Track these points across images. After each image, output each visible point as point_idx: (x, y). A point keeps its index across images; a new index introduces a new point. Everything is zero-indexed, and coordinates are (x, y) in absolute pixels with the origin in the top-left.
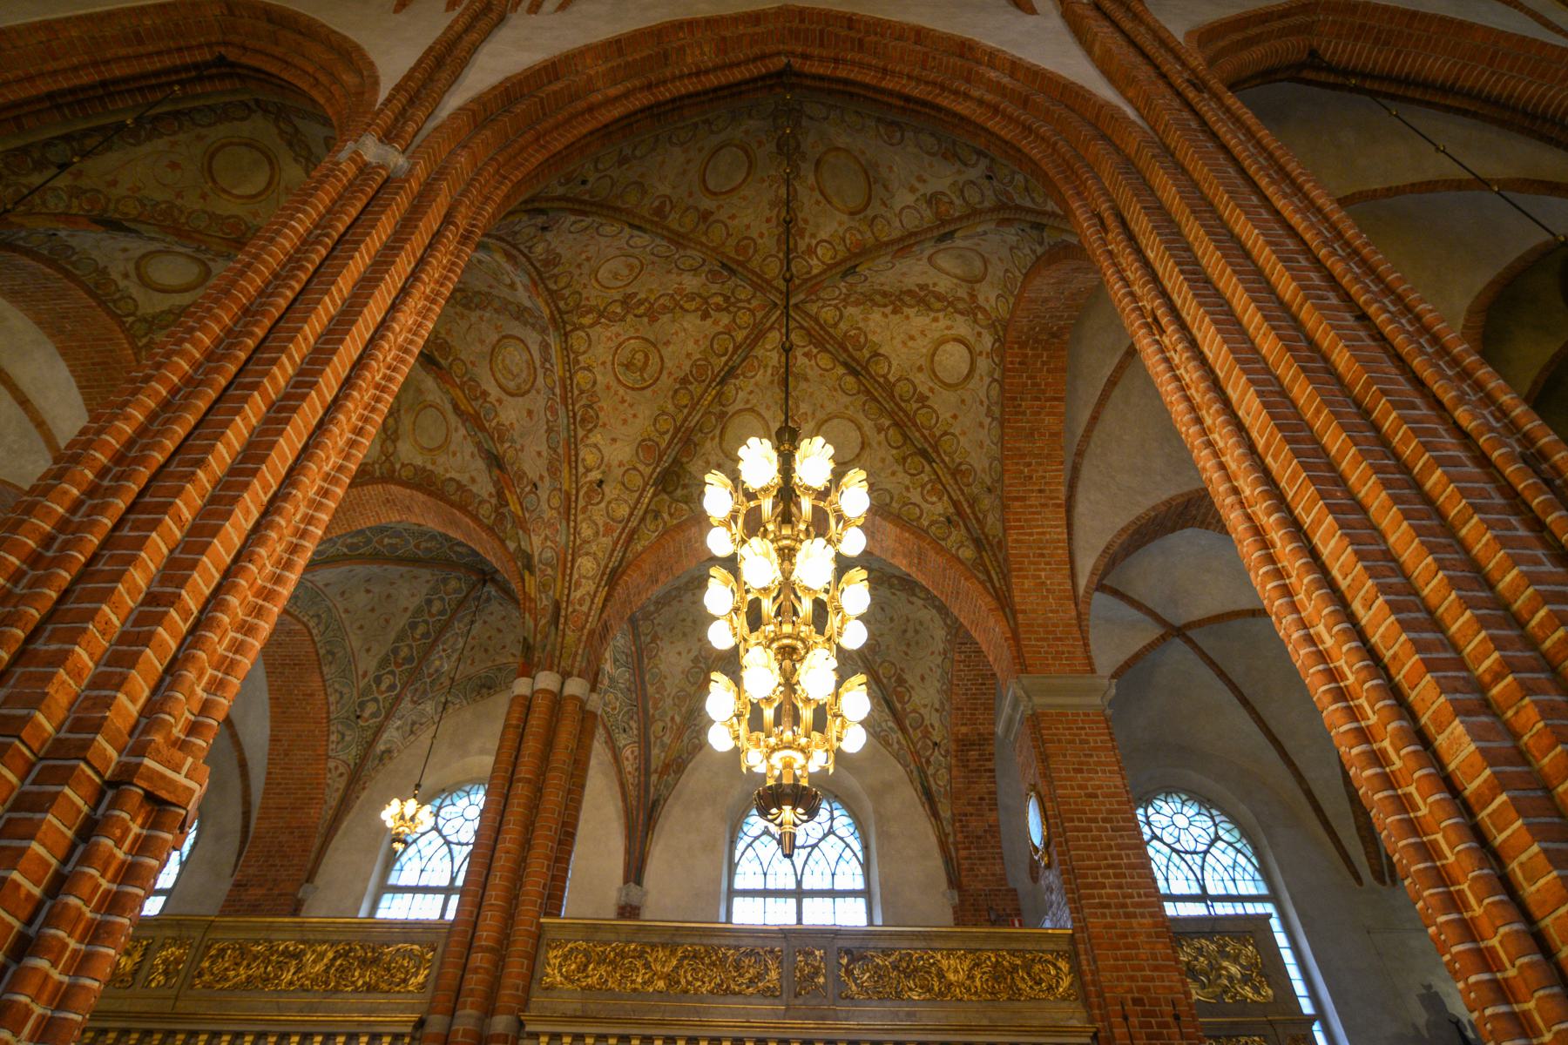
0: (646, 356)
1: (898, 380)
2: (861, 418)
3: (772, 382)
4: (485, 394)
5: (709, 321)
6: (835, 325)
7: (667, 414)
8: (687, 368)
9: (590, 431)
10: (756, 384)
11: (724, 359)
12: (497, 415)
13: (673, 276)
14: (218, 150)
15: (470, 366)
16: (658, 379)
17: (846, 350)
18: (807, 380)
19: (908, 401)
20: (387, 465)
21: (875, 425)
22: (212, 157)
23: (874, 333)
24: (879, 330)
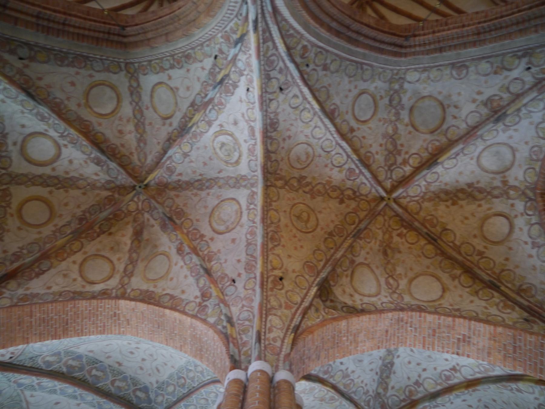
1: (462, 244)
2: (440, 273)
3: (379, 251)
4: (202, 236)
5: (344, 205)
6: (417, 213)
7: (321, 251)
8: (332, 226)
9: (276, 246)
10: (371, 249)
11: (353, 226)
12: (209, 247)
14: (97, 85)
15: (195, 222)
17: (426, 227)
18: (400, 252)
19: (471, 256)
20: (122, 290)
21: (451, 276)
22: (92, 88)
23: (442, 217)
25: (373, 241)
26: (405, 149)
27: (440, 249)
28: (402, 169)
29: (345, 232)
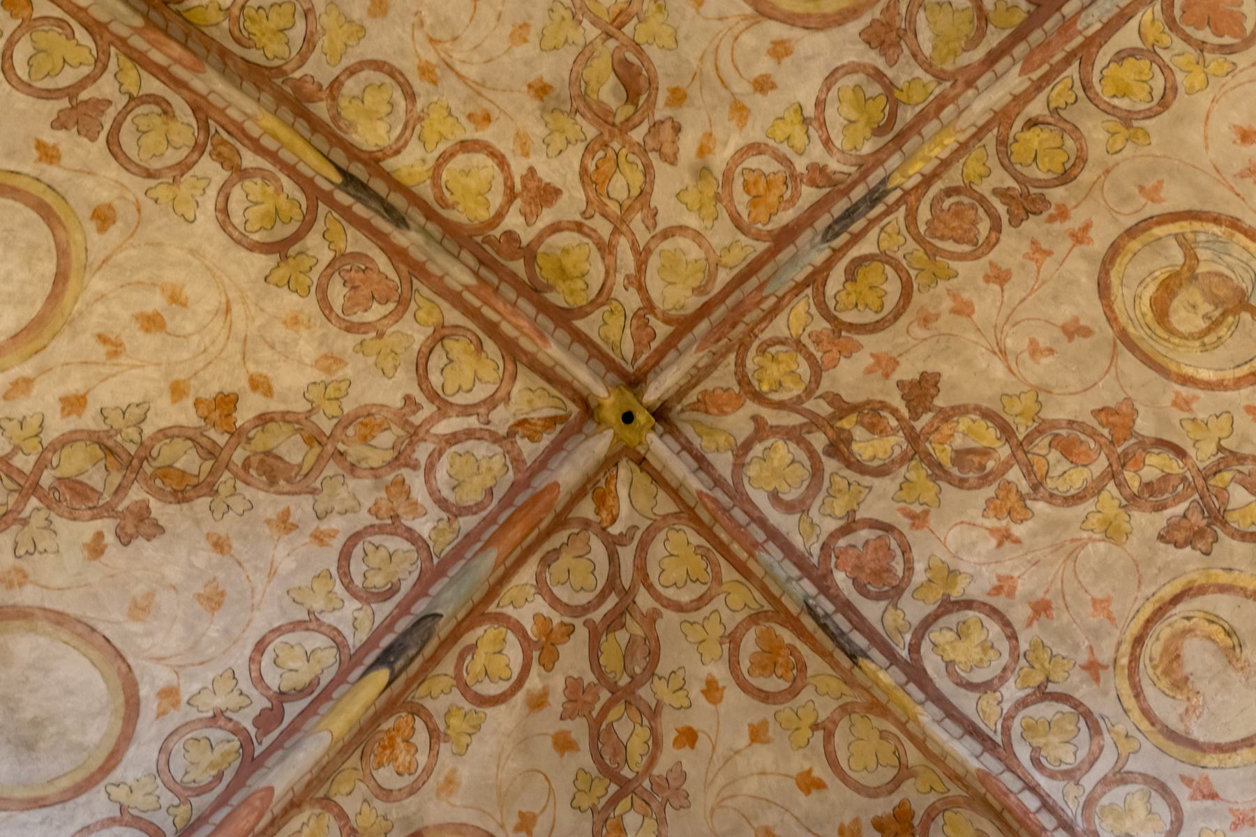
0: (1161, 312)
1: (184, 167)
3: (678, 97)
5: (908, 371)
6: (440, 335)
7: (1111, 111)
10: (740, 111)
11: (866, 247)
13: (1027, 584)
16: (1131, 233)
17: (397, 254)
18: (541, 90)
19: (135, 100)
23: (294, 321)
24: (279, 332)
25: (720, 159)
26: (549, 721)
27: (315, 125)
28: (555, 602)
29: (924, 214)
